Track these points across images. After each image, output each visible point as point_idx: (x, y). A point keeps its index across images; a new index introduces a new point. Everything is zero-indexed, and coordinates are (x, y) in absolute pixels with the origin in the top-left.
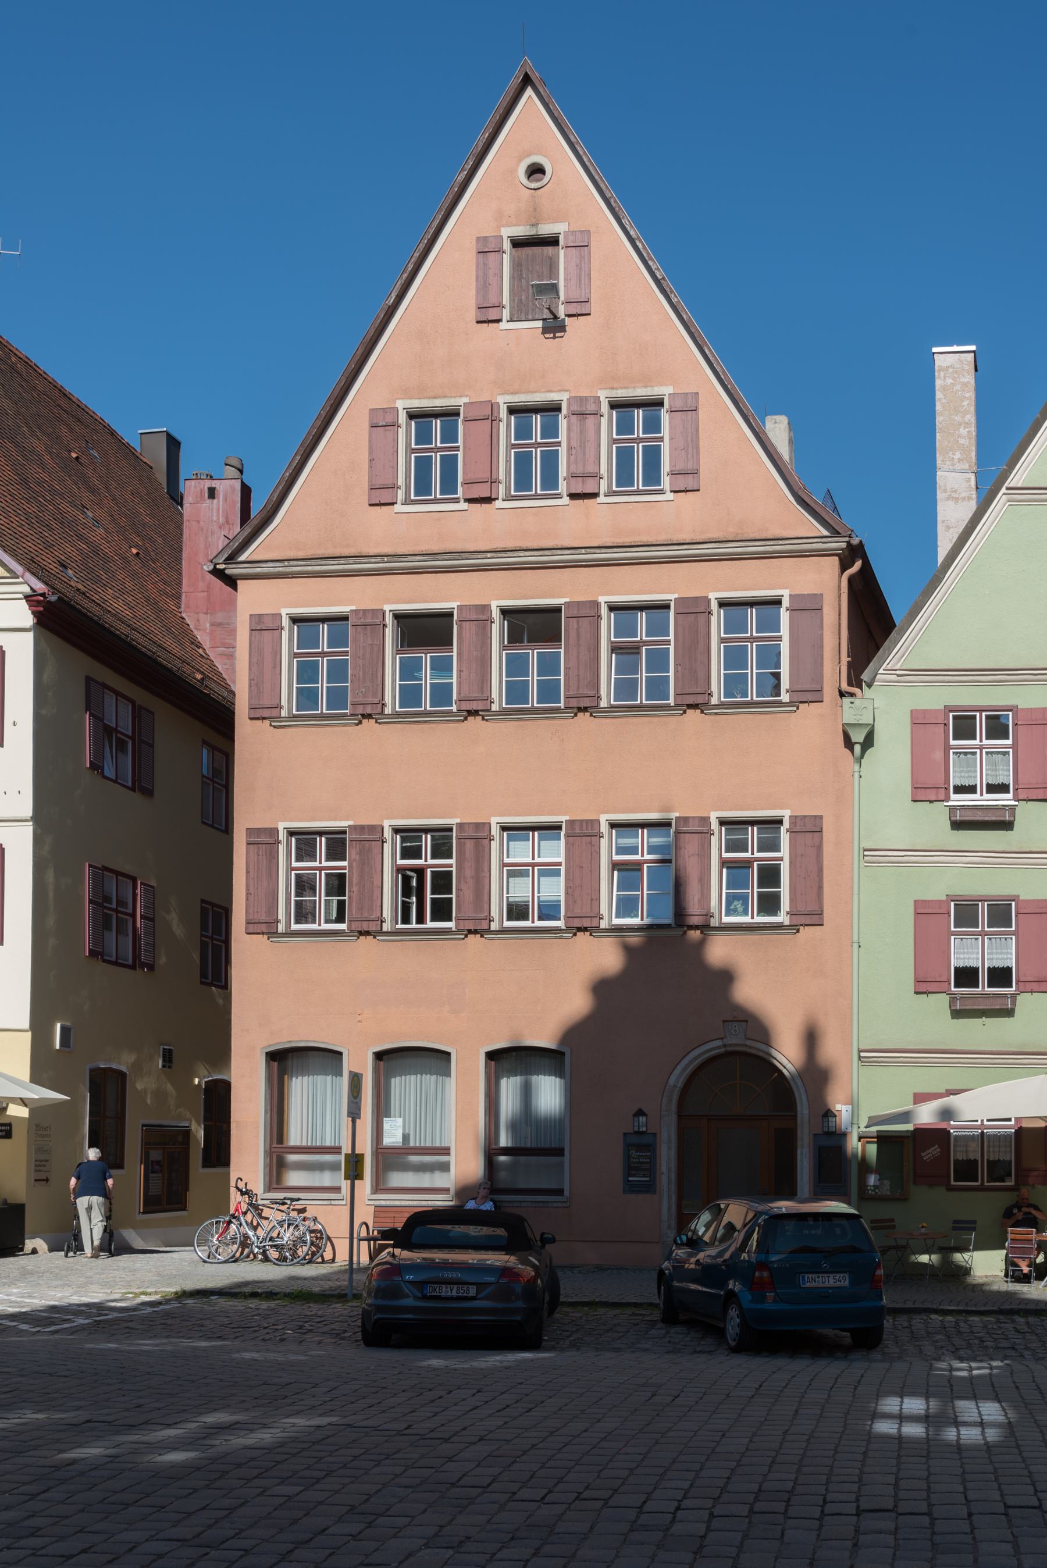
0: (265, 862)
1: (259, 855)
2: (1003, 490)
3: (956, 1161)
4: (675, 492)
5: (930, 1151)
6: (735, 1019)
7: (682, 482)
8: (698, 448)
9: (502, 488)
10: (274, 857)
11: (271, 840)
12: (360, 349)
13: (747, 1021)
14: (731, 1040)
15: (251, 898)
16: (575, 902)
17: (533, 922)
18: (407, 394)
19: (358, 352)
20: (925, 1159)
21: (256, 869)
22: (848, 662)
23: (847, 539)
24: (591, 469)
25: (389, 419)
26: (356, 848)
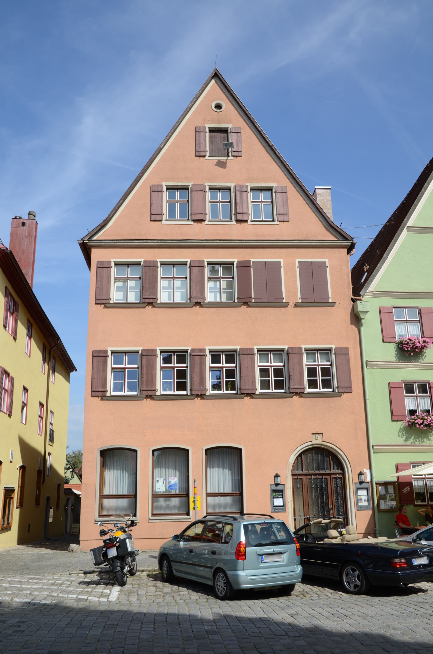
0: (101, 365)
1: (98, 362)
2: (406, 228)
3: (416, 493)
4: (280, 221)
5: (406, 489)
6: (317, 433)
7: (282, 218)
8: (288, 206)
9: (207, 216)
10: (106, 362)
11: (105, 355)
12: (149, 163)
13: (322, 434)
14: (315, 442)
15: (94, 381)
16: (245, 382)
17: (223, 391)
18: (166, 180)
19: (148, 164)
20: (404, 492)
21: (97, 367)
22: (352, 288)
23: (351, 242)
24: (245, 211)
25: (160, 189)
26: (145, 358)
